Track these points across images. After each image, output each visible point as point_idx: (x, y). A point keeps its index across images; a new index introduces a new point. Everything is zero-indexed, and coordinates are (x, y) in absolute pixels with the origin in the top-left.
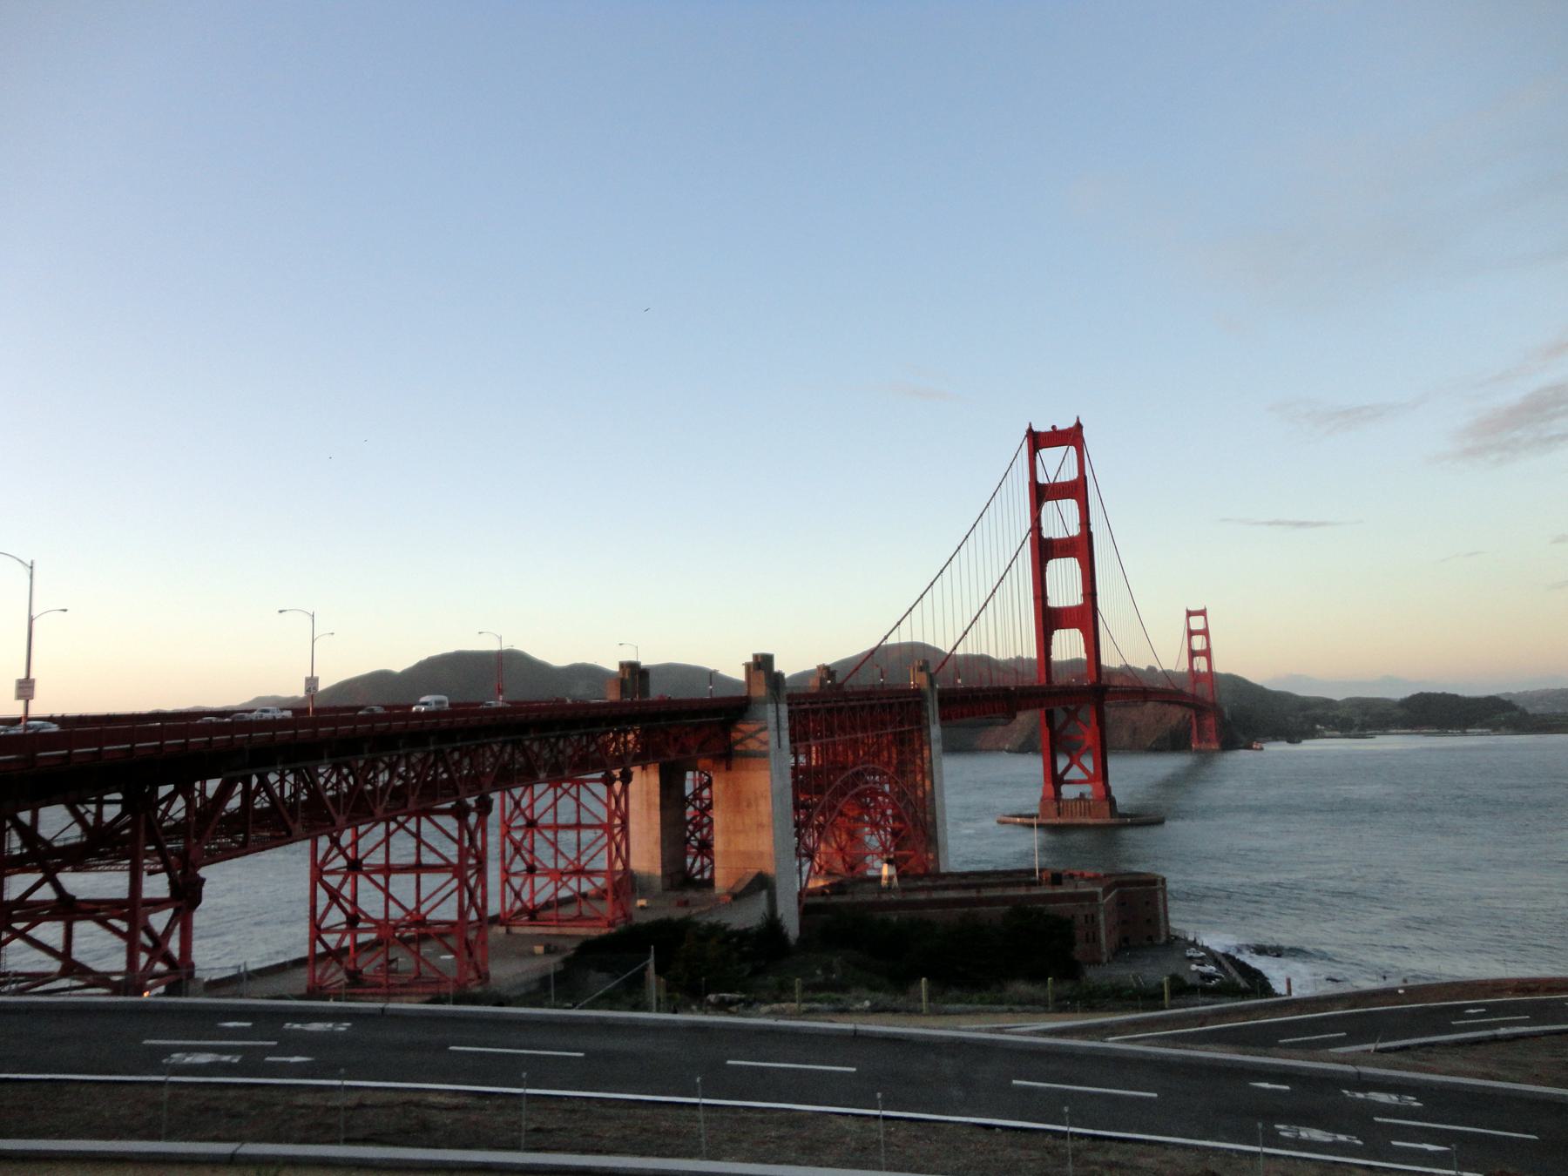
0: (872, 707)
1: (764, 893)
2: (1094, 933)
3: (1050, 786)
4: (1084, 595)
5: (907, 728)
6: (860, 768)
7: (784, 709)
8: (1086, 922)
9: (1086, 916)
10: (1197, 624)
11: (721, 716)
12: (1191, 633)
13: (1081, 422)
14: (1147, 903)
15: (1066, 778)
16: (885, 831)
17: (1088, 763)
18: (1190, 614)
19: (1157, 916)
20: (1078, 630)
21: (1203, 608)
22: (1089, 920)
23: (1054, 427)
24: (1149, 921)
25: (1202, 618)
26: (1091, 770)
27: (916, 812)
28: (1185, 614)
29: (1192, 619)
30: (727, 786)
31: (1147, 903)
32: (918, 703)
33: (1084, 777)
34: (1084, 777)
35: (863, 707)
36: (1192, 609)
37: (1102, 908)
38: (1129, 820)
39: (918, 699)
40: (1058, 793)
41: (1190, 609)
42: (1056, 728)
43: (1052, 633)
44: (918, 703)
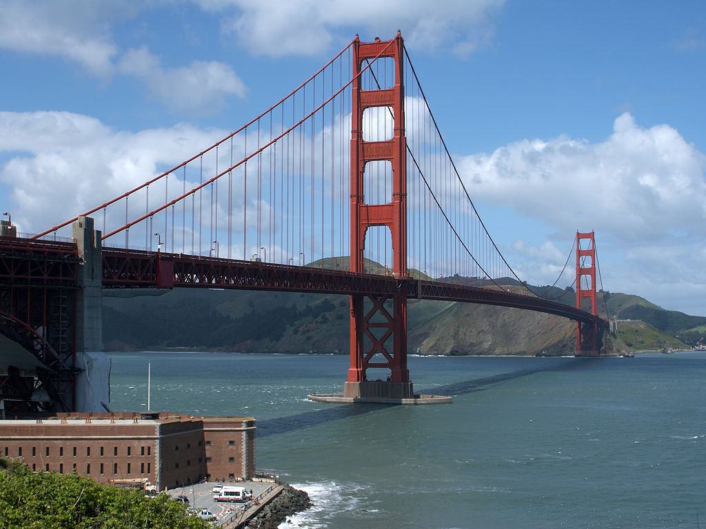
2: (149, 464)
8: (143, 454)
9: (143, 448)
22: (146, 452)
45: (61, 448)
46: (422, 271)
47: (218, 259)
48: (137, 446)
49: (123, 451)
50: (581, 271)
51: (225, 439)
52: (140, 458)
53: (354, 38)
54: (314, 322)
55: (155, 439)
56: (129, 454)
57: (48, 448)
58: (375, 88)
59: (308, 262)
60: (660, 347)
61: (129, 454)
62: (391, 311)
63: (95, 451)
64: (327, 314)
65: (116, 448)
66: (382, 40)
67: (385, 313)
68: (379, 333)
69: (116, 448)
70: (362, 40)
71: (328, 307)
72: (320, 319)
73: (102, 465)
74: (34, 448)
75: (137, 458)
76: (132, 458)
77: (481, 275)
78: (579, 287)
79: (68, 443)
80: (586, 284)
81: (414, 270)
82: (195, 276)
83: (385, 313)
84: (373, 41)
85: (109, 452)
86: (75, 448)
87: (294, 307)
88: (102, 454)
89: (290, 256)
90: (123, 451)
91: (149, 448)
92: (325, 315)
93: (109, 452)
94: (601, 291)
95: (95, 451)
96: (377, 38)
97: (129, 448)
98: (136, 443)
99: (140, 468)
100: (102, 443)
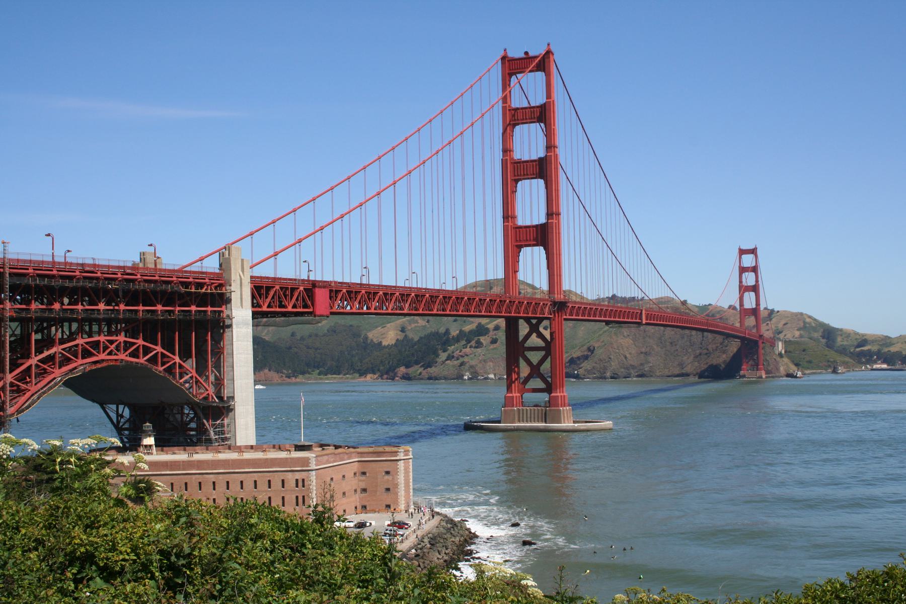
8: (297, 486)
9: (297, 480)
10: (748, 261)
12: (743, 270)
13: (553, 48)
14: (388, 473)
18: (742, 252)
19: (396, 486)
21: (754, 247)
22: (300, 484)
23: (526, 53)
24: (388, 490)
25: (752, 256)
28: (737, 251)
29: (744, 256)
31: (388, 473)
36: (744, 247)
41: (742, 248)
42: (521, 338)
45: (214, 483)
46: (579, 292)
47: (369, 285)
48: (291, 478)
49: (276, 484)
50: (743, 289)
51: (381, 469)
52: (294, 490)
53: (502, 53)
54: (468, 347)
56: (283, 487)
57: (200, 483)
58: (526, 105)
59: (461, 285)
60: (830, 366)
61: (283, 487)
62: (547, 333)
64: (482, 339)
65: (269, 481)
66: (531, 54)
67: (540, 336)
68: (535, 357)
69: (269, 481)
70: (511, 54)
71: (481, 331)
72: (473, 343)
75: (292, 491)
76: (286, 490)
77: (638, 295)
78: (741, 304)
79: (221, 477)
80: (749, 301)
81: (570, 291)
82: (345, 303)
83: (540, 336)
84: (522, 55)
86: (228, 483)
87: (447, 332)
88: (256, 487)
89: (443, 281)
90: (276, 484)
91: (303, 480)
92: (479, 339)
94: (766, 309)
96: (526, 53)
98: (290, 475)
99: (295, 501)
100: (256, 477)
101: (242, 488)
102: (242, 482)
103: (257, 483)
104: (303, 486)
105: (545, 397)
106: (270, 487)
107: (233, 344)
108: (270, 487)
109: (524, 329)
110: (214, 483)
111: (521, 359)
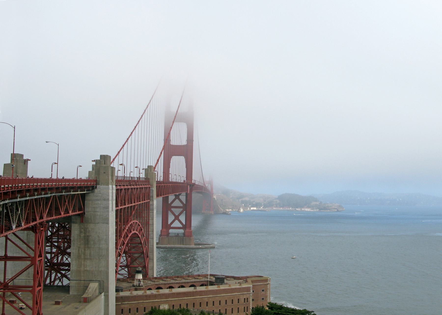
0: (137, 188)
1: (103, 294)
2: (247, 307)
3: (165, 230)
4: (188, 141)
5: (146, 201)
6: (132, 222)
7: (114, 187)
11: (85, 191)
14: (263, 290)
15: (172, 226)
16: (128, 255)
17: (183, 218)
20: (183, 157)
22: (246, 301)
24: (263, 299)
26: (184, 222)
27: (146, 245)
30: (81, 232)
31: (263, 290)
32: (149, 188)
33: (181, 226)
34: (181, 226)
35: (135, 188)
37: (251, 294)
38: (200, 246)
39: (150, 186)
40: (168, 234)
42: (169, 203)
43: (171, 158)
44: (149, 188)
45: (207, 302)
49: (236, 301)
55: (250, 293)
56: (238, 303)
57: (200, 303)
61: (238, 303)
63: (223, 302)
65: (232, 300)
69: (232, 300)
73: (226, 309)
74: (194, 304)
85: (229, 303)
86: (213, 302)
88: (226, 304)
90: (236, 301)
91: (247, 298)
93: (229, 303)
95: (223, 302)
97: (238, 299)
101: (220, 304)
102: (220, 301)
103: (227, 301)
104: (247, 302)
105: (182, 231)
106: (232, 303)
107: (153, 219)
108: (232, 303)
109: (171, 197)
110: (207, 302)
111: (169, 211)
